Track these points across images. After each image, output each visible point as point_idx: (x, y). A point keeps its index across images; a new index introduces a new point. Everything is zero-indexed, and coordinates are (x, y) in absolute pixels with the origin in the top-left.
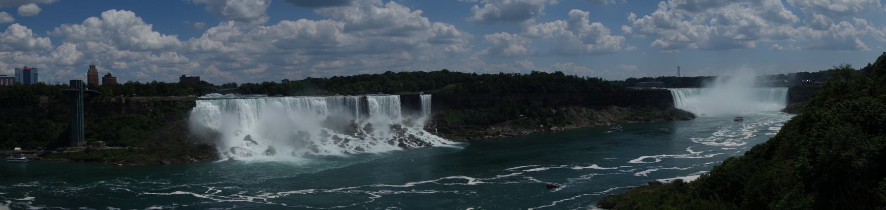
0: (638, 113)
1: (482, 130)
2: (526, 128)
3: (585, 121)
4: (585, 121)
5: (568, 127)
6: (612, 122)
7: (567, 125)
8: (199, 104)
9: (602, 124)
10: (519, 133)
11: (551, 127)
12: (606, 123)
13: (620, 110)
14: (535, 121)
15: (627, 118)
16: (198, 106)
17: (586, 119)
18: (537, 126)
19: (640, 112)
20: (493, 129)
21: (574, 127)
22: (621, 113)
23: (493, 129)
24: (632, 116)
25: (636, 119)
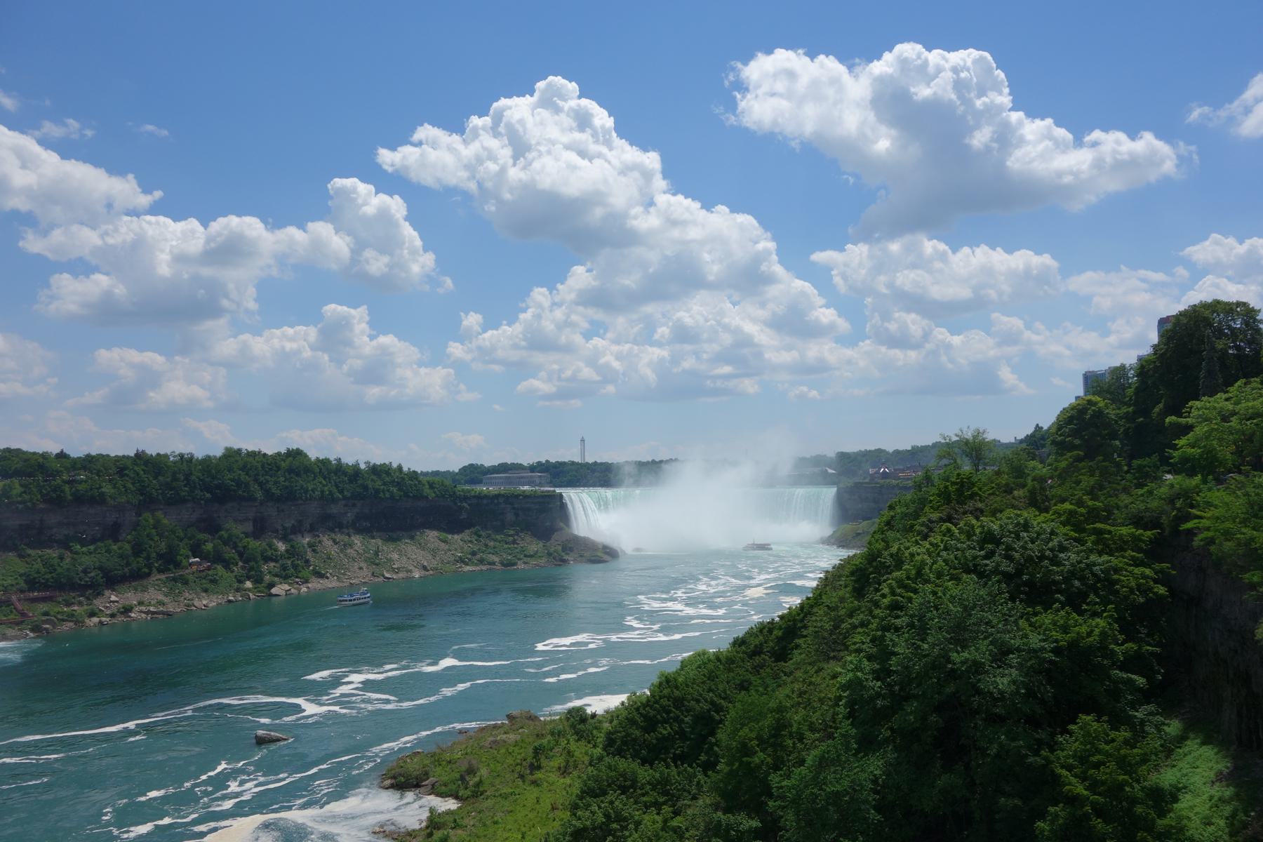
0: (486, 545)
1: (80, 603)
2: (206, 591)
3: (361, 568)
4: (361, 568)
5: (316, 584)
6: (425, 568)
7: (313, 579)
9: (401, 575)
11: (272, 585)
12: (411, 571)
13: (445, 541)
14: (232, 572)
15: (461, 560)
17: (362, 565)
18: (236, 585)
19: (491, 544)
21: (331, 583)
22: (447, 547)
23: (113, 598)
24: (474, 554)
25: (481, 561)
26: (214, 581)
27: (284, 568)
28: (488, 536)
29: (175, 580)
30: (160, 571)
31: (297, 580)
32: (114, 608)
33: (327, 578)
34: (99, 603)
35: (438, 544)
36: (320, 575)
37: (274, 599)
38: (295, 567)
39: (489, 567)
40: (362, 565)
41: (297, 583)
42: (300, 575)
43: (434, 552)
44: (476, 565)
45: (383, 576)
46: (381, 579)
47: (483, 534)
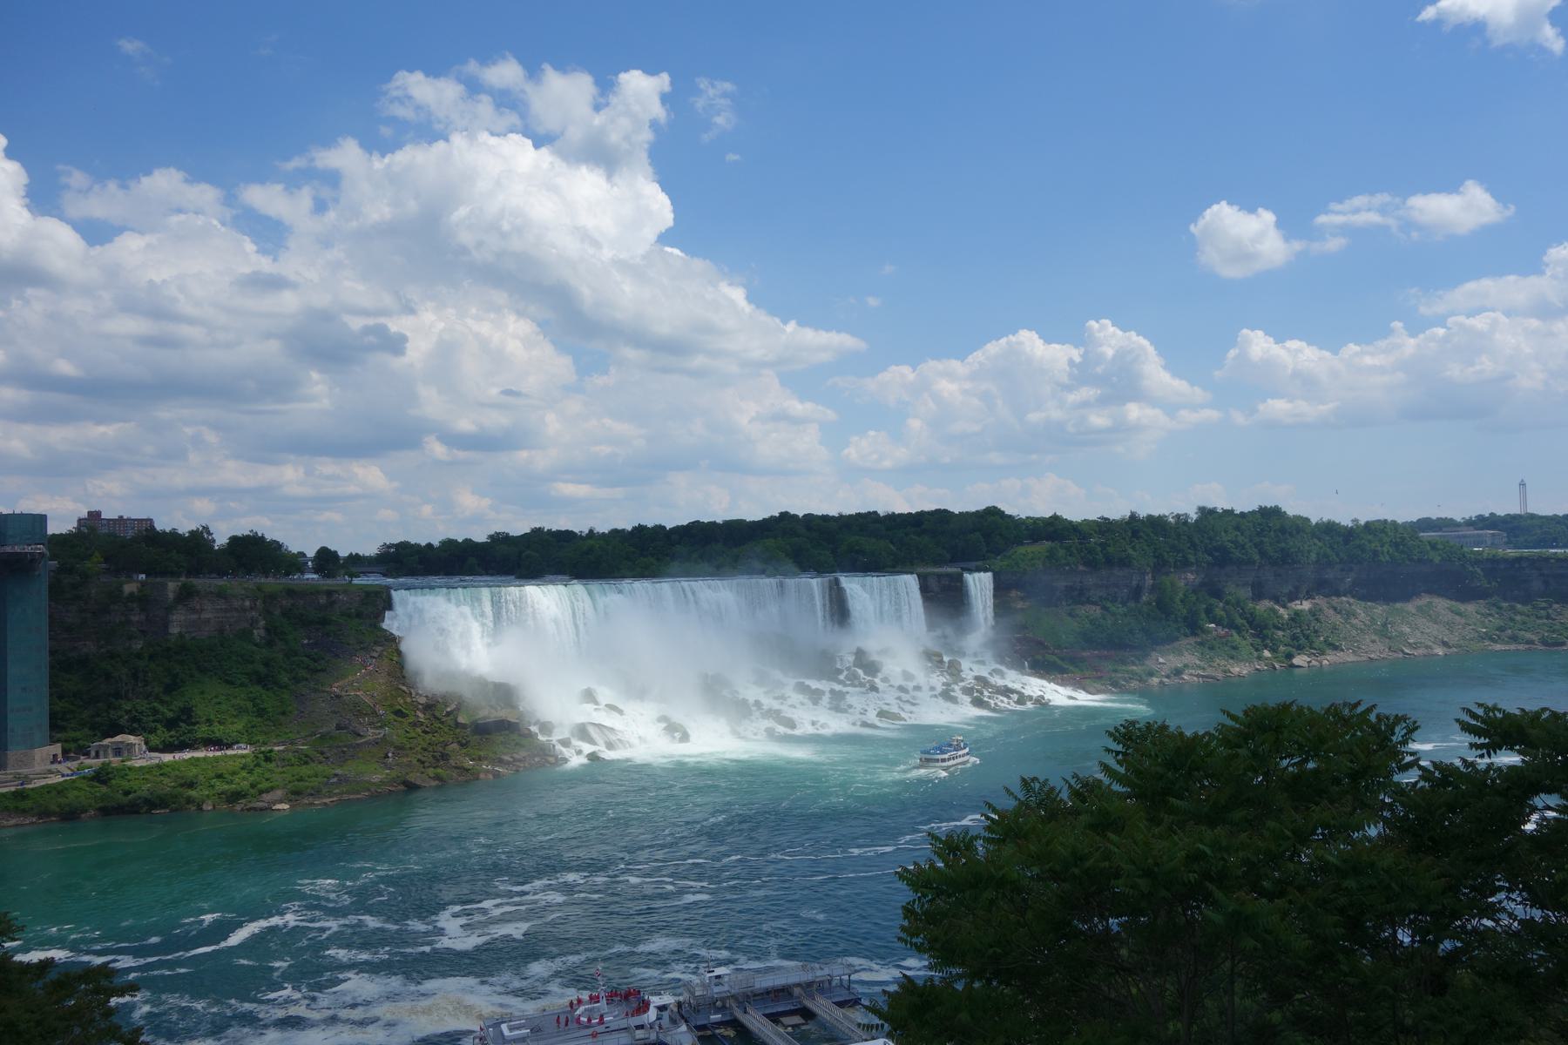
0: (1512, 620)
2: (1232, 658)
3: (1373, 641)
4: (1373, 641)
5: (1330, 659)
6: (1445, 644)
7: (1328, 651)
8: (404, 602)
9: (1421, 651)
10: (1225, 672)
11: (1290, 656)
12: (1430, 647)
13: (1459, 614)
15: (1482, 638)
16: (398, 608)
17: (1374, 637)
18: (1256, 654)
19: (1518, 618)
20: (1161, 660)
21: (1349, 657)
23: (1161, 660)
25: (1514, 639)
26: (1235, 648)
27: (1294, 638)
28: (1512, 608)
29: (1201, 644)
30: (1186, 636)
31: (1313, 651)
32: (1166, 670)
33: (1343, 650)
34: (1150, 664)
35: (1450, 616)
36: (1336, 648)
37: (1297, 671)
38: (1307, 637)
39: (1527, 646)
40: (1374, 637)
41: (1314, 654)
42: (1314, 646)
43: (1450, 626)
44: (1507, 643)
45: (1403, 651)
46: (1401, 655)
47: (1505, 605)
